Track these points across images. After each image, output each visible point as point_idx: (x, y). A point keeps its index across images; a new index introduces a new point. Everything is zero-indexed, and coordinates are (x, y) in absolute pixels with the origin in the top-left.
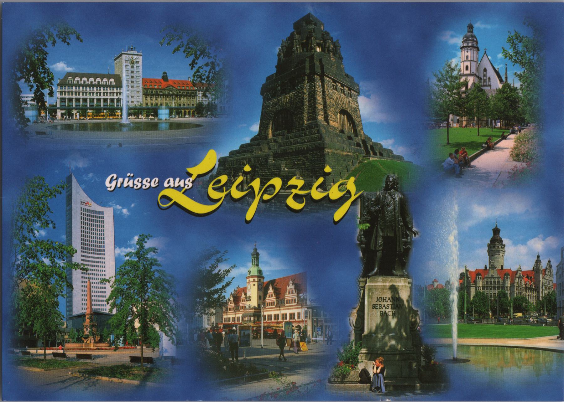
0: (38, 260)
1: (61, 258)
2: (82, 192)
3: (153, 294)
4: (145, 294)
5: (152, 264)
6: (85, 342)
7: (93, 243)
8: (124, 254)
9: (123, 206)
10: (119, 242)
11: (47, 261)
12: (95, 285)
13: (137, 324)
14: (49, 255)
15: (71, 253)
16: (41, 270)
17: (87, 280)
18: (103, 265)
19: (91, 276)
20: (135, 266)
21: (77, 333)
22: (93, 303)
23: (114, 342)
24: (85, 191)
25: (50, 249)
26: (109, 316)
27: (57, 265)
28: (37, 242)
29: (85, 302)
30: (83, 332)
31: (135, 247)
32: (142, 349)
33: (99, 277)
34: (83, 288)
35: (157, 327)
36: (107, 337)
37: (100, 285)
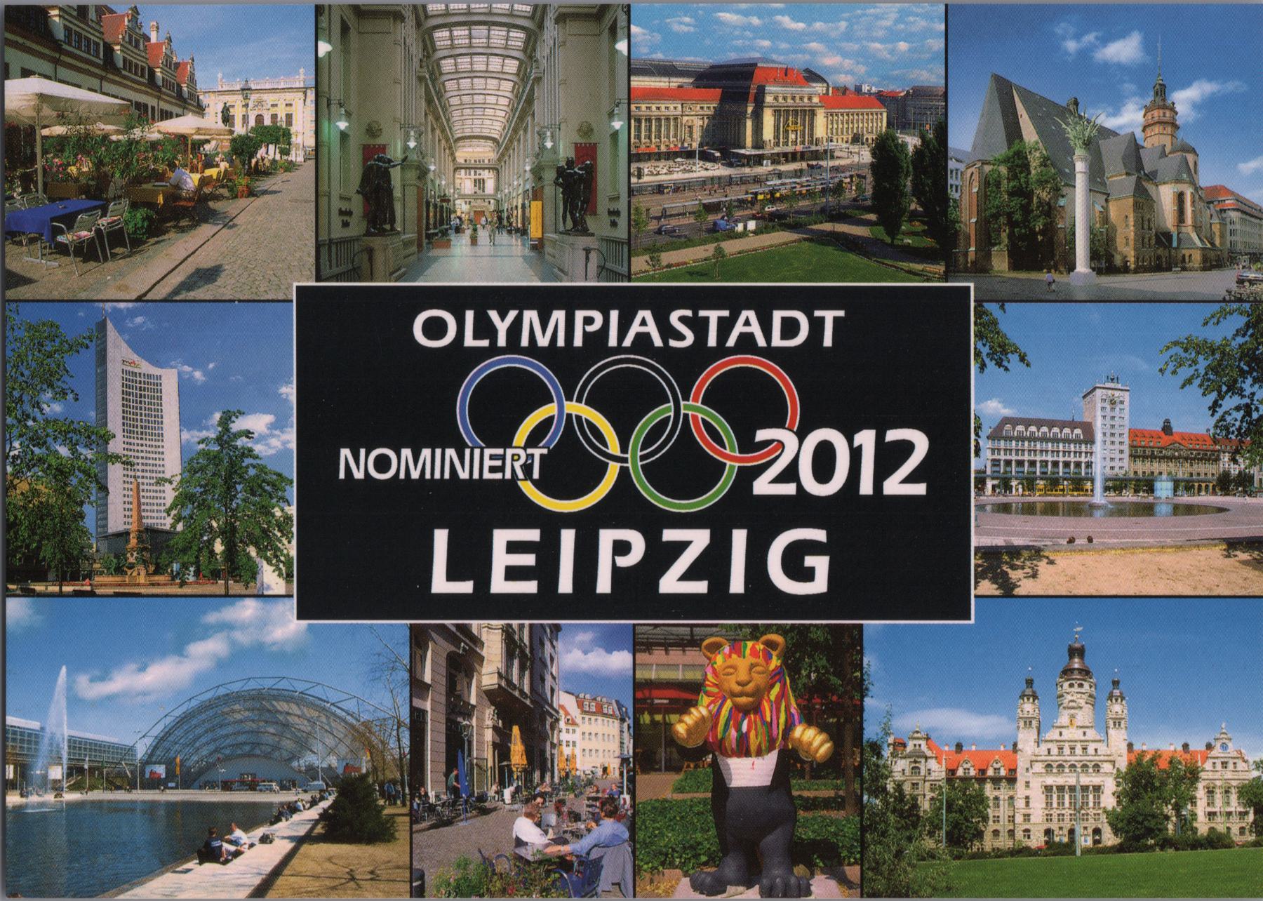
8: (197, 440)
9: (195, 366)
10: (186, 421)
13: (219, 547)
15: (106, 438)
19: (139, 474)
20: (214, 459)
23: (178, 573)
24: (129, 343)
26: (170, 534)
32: (226, 584)
34: (126, 492)
35: (252, 551)
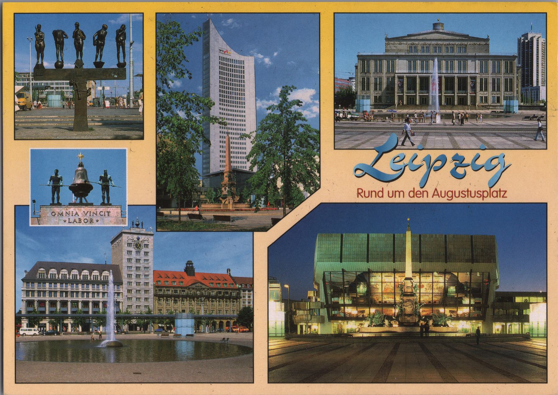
0: (172, 113)
1: (197, 111)
2: (220, 39)
3: (296, 150)
4: (288, 150)
5: (296, 118)
6: (223, 202)
7: (232, 93)
8: (267, 107)
9: (265, 55)
10: (260, 94)
11: (182, 114)
12: (235, 141)
13: (280, 184)
14: (185, 108)
15: (209, 105)
16: (176, 124)
17: (226, 135)
18: (243, 118)
19: (230, 131)
20: (277, 120)
21: (214, 193)
22: (232, 160)
23: (254, 203)
24: (224, 38)
25: (186, 101)
26: (249, 174)
27: (194, 119)
28: (171, 93)
29: (224, 154)
30: (222, 192)
31: (278, 100)
32: (284, 210)
33: (239, 132)
34: (221, 144)
35: (301, 187)
36: (247, 197)
37: (239, 141)
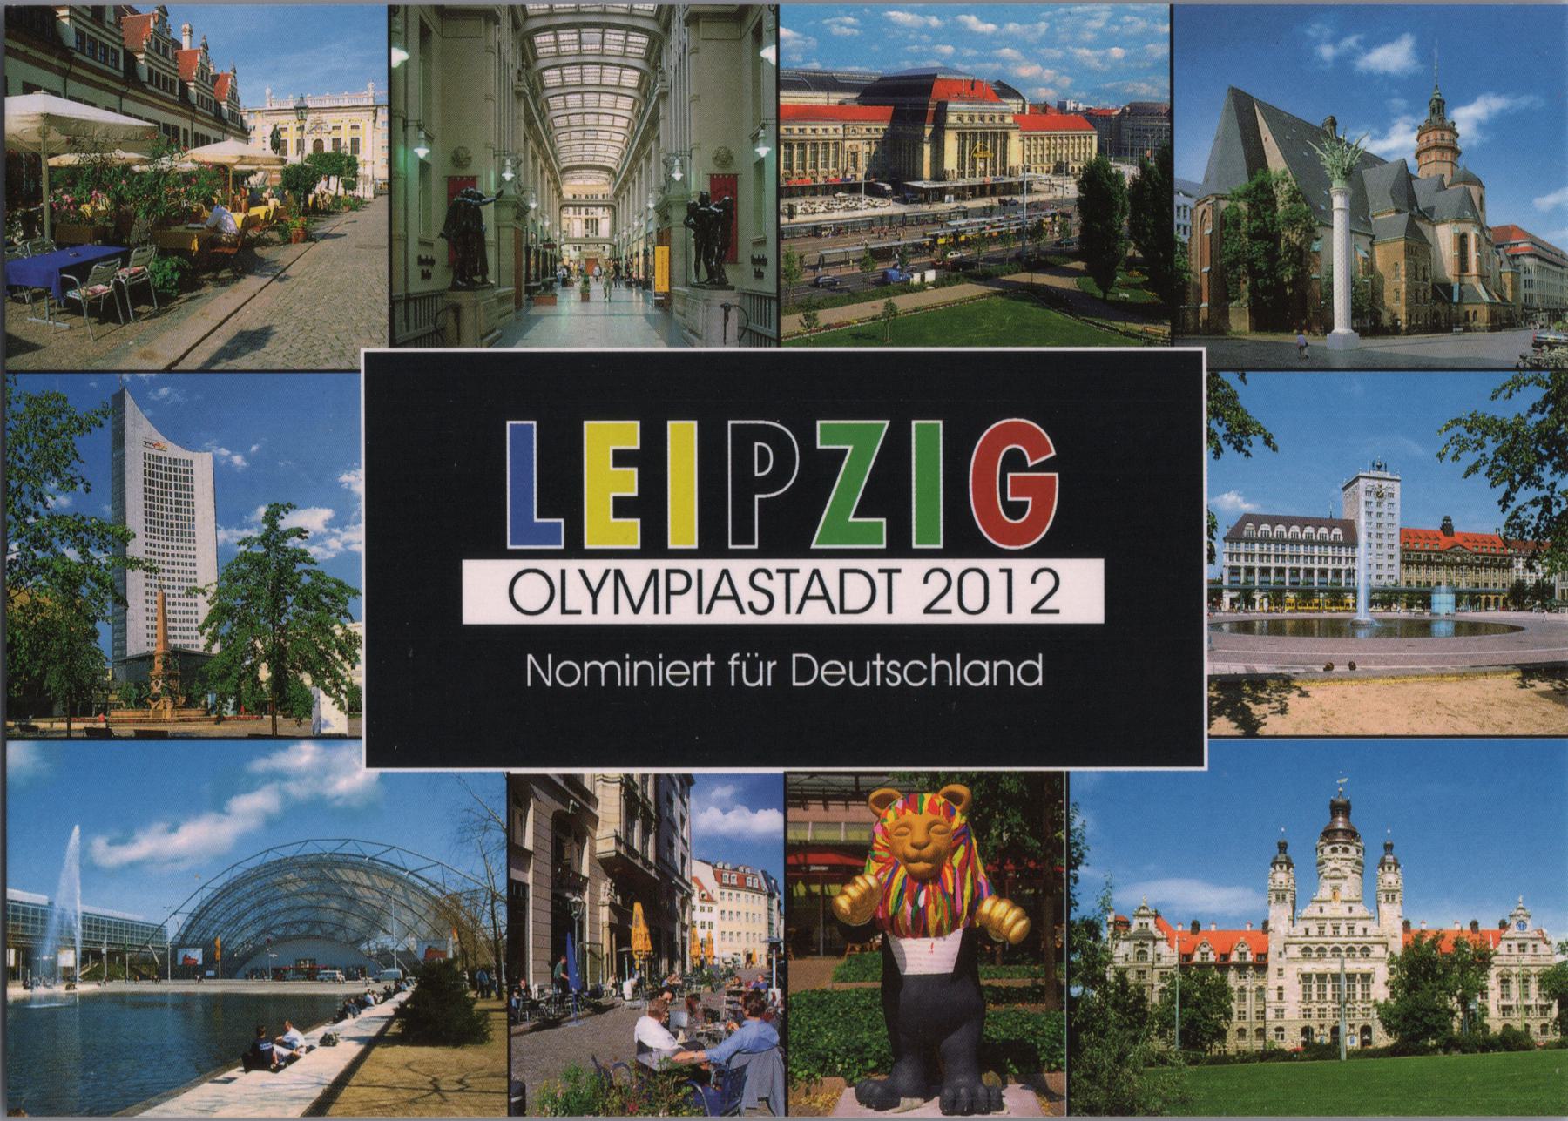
2: (146, 423)
3: (297, 616)
7: (171, 514)
9: (234, 450)
10: (224, 518)
12: (177, 600)
13: (264, 673)
15: (124, 538)
19: (166, 583)
20: (258, 563)
21: (136, 691)
23: (214, 707)
26: (203, 658)
32: (274, 719)
35: (307, 679)
37: (185, 600)
